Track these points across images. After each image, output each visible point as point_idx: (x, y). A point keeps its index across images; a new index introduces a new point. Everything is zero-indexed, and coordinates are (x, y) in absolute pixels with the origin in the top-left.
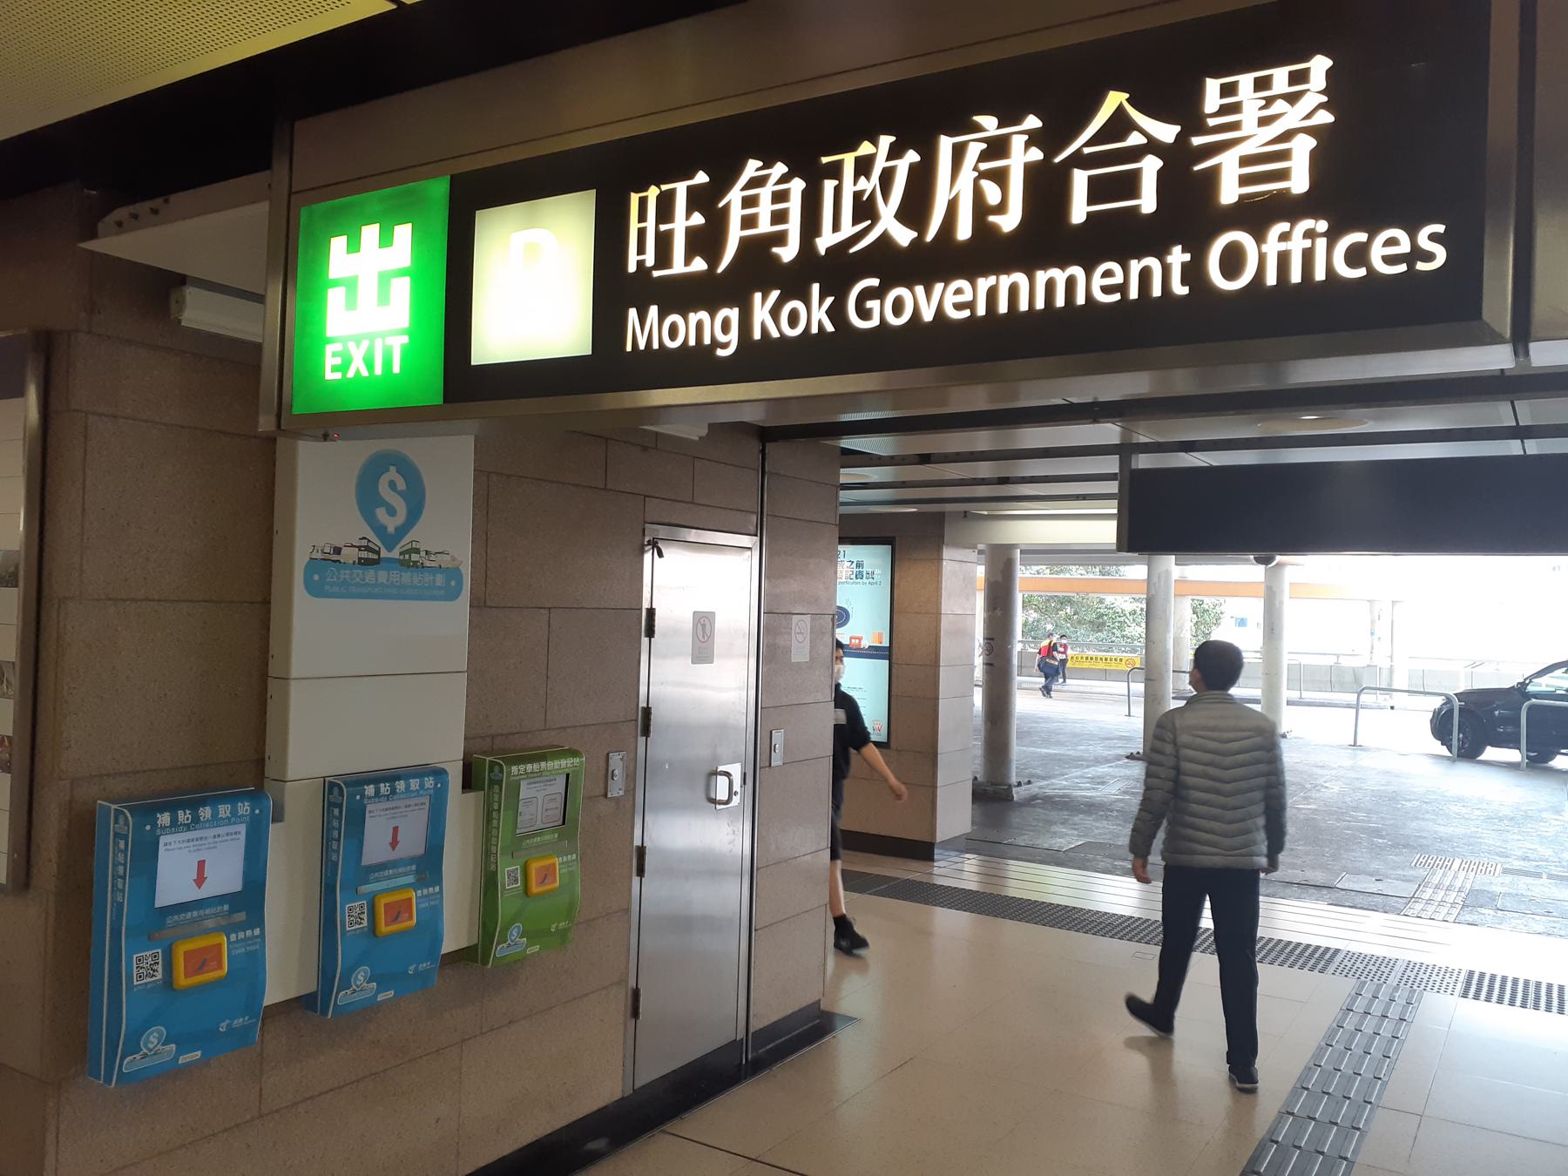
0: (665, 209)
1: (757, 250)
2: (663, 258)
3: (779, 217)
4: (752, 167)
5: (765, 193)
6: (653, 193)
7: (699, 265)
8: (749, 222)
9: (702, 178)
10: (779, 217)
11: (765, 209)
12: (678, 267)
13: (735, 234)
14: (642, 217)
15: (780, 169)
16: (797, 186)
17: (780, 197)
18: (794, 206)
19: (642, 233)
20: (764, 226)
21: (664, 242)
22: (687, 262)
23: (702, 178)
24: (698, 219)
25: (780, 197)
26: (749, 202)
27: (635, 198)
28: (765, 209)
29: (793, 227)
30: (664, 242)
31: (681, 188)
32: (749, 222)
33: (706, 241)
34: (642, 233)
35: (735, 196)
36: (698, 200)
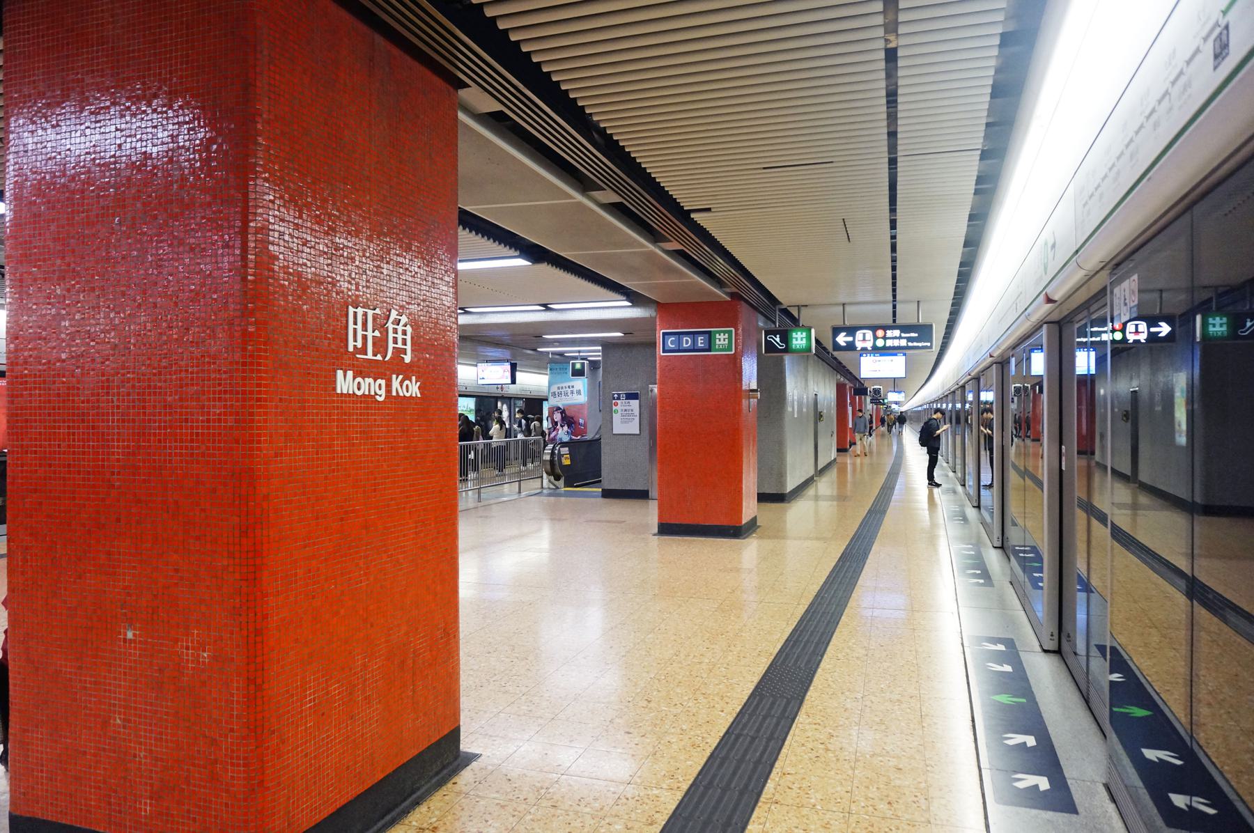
1: (399, 352)
2: (364, 350)
3: (404, 342)
6: (360, 311)
7: (379, 357)
8: (395, 341)
9: (378, 311)
10: (404, 342)
11: (400, 336)
12: (370, 356)
13: (391, 345)
14: (355, 323)
16: (409, 329)
17: (404, 333)
19: (355, 330)
20: (400, 345)
21: (365, 338)
22: (375, 355)
23: (378, 311)
24: (377, 334)
25: (404, 333)
26: (395, 331)
28: (400, 336)
29: (408, 347)
30: (365, 338)
31: (370, 313)
32: (395, 341)
33: (380, 345)
34: (355, 330)
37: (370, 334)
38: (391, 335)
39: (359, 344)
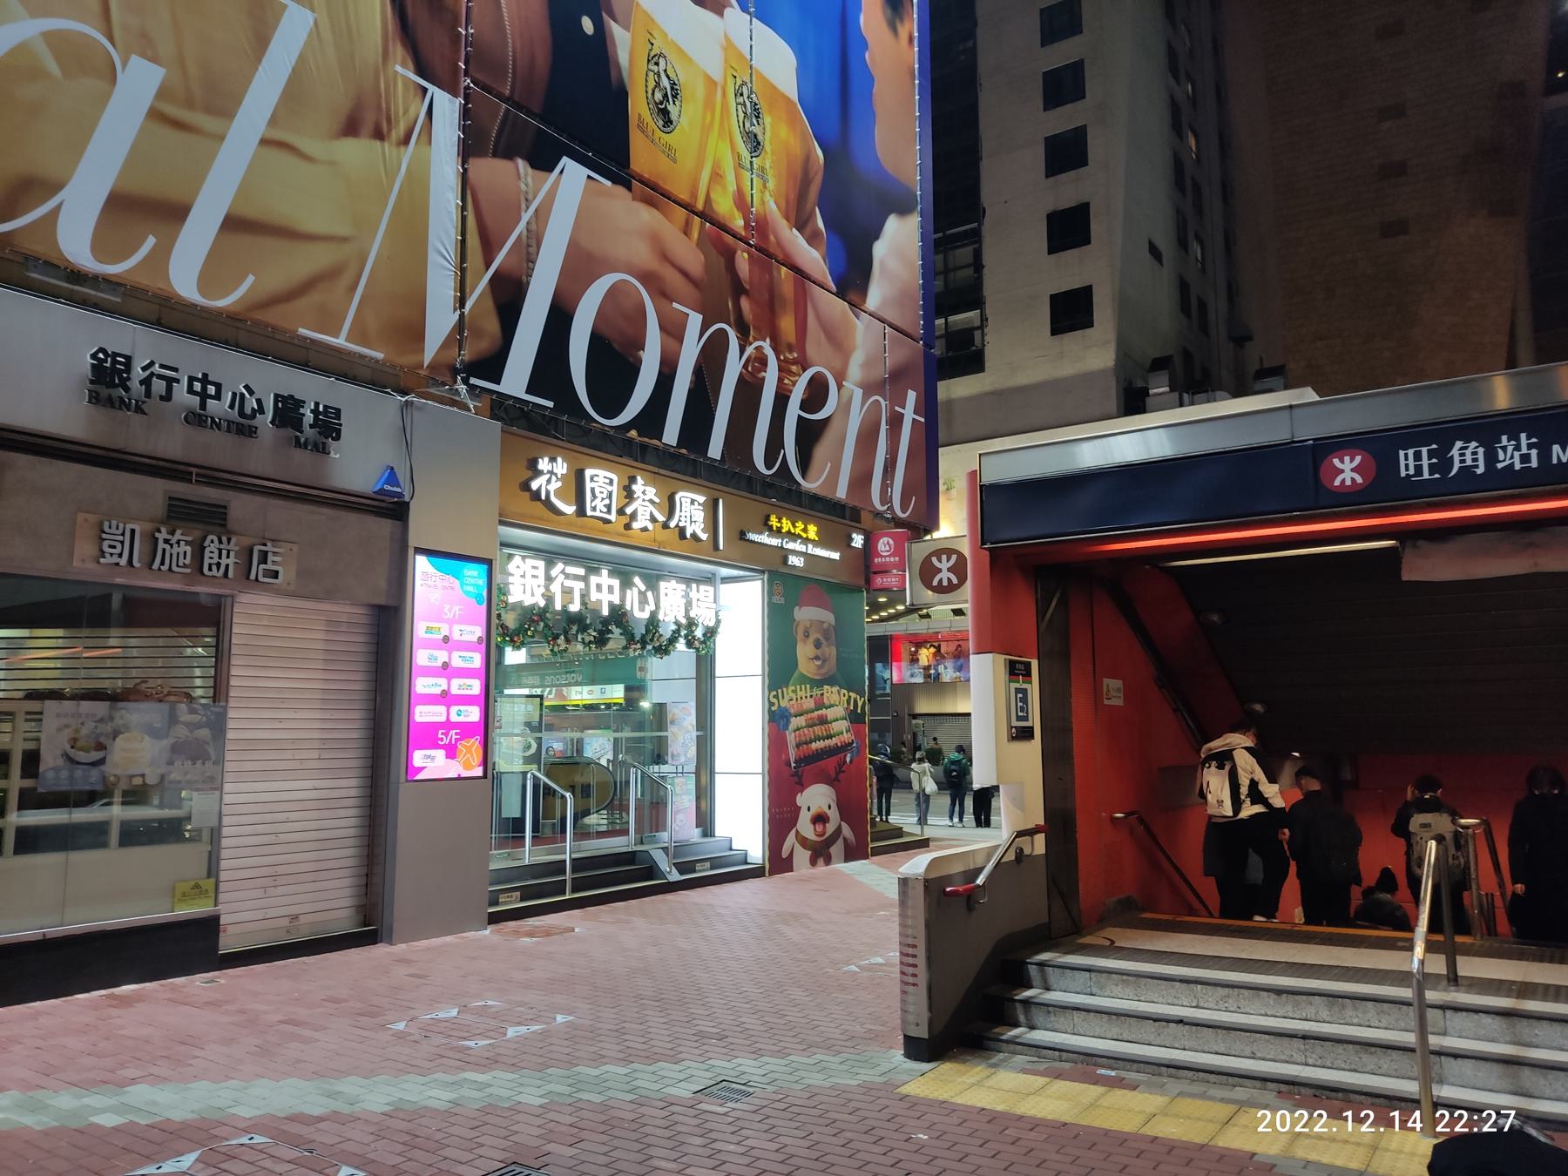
0: (1418, 456)
3: (1475, 460)
4: (1459, 444)
5: (1468, 452)
6: (1411, 452)
8: (1463, 461)
10: (1475, 460)
12: (1426, 476)
15: (1474, 444)
16: (1481, 450)
18: (1481, 456)
20: (1469, 463)
21: (1419, 469)
25: (1474, 453)
26: (1462, 455)
27: (1402, 453)
29: (1481, 463)
30: (1419, 469)
31: (1424, 450)
35: (1455, 452)
36: (1431, 454)
37: (1425, 462)
38: (1457, 460)
39: (1412, 472)
